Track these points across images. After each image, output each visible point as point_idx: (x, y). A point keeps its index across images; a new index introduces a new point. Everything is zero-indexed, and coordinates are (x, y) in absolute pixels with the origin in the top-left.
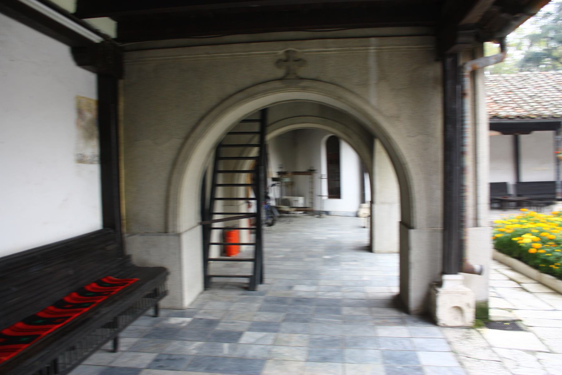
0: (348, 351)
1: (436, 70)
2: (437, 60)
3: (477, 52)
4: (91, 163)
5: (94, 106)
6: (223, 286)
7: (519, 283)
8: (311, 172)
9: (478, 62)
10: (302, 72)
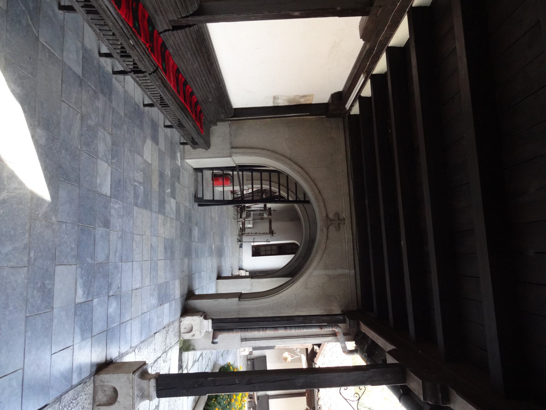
0: (169, 261)
1: (336, 310)
2: (342, 311)
3: (349, 335)
4: (274, 103)
5: (308, 102)
6: (196, 180)
8: (272, 232)
9: (341, 336)
10: (332, 229)
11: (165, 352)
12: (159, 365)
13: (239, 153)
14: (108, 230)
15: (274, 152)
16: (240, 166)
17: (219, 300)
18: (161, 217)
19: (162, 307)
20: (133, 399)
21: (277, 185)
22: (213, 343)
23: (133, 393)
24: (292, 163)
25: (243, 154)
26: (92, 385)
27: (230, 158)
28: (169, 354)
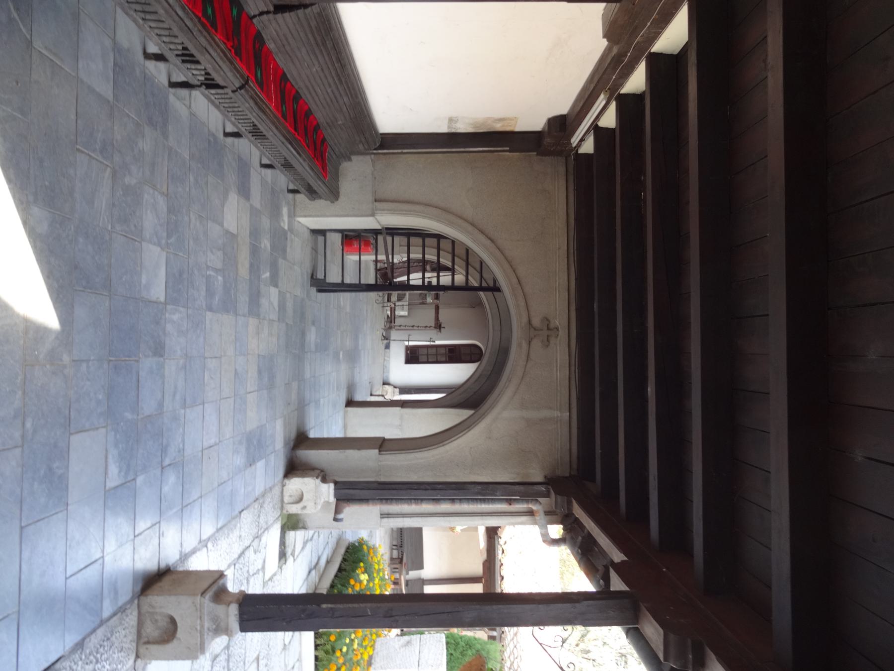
0: (265, 392)
2: (545, 477)
3: (552, 515)
4: (449, 127)
5: (508, 129)
6: (315, 250)
7: (315, 567)
8: (438, 326)
9: (540, 517)
10: (537, 344)
11: (258, 537)
12: (246, 559)
13: (388, 210)
14: (162, 359)
15: (447, 211)
16: (387, 229)
17: (348, 451)
18: (253, 321)
19: (253, 467)
20: (202, 635)
21: (450, 256)
22: (335, 520)
23: (202, 626)
24: (476, 231)
25: (393, 212)
26: (135, 613)
27: (371, 219)
28: (264, 539)
